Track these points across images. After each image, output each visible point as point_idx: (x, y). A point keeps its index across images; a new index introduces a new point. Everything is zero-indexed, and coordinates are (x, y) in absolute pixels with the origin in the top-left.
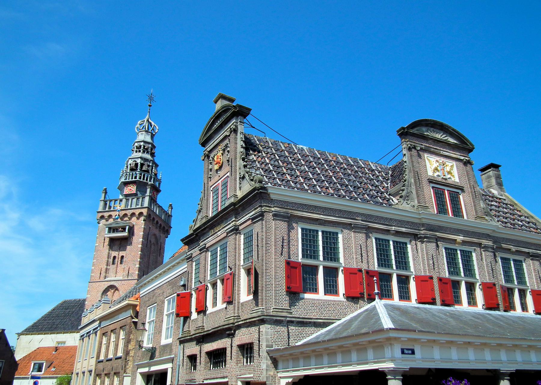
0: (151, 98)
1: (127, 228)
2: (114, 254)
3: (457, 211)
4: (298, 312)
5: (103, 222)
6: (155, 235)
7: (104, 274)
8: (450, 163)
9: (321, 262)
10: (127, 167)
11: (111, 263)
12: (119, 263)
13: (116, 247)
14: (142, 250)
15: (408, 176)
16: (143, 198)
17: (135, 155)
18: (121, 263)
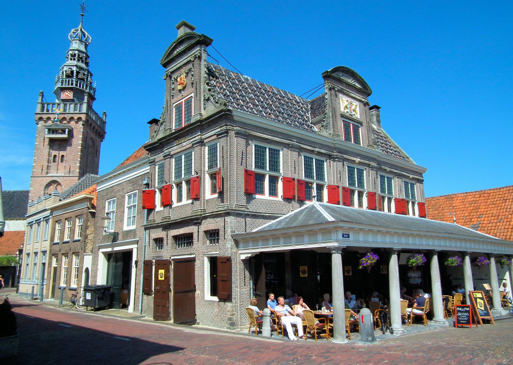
0: (83, 8)
1: (67, 131)
2: (54, 153)
3: (357, 140)
4: (252, 207)
5: (41, 123)
6: (92, 138)
7: (46, 171)
8: (355, 103)
9: (267, 172)
10: (63, 73)
11: (52, 161)
12: (60, 161)
13: (56, 147)
14: (82, 151)
15: (328, 111)
16: (81, 104)
17: (69, 62)
18: (62, 161)
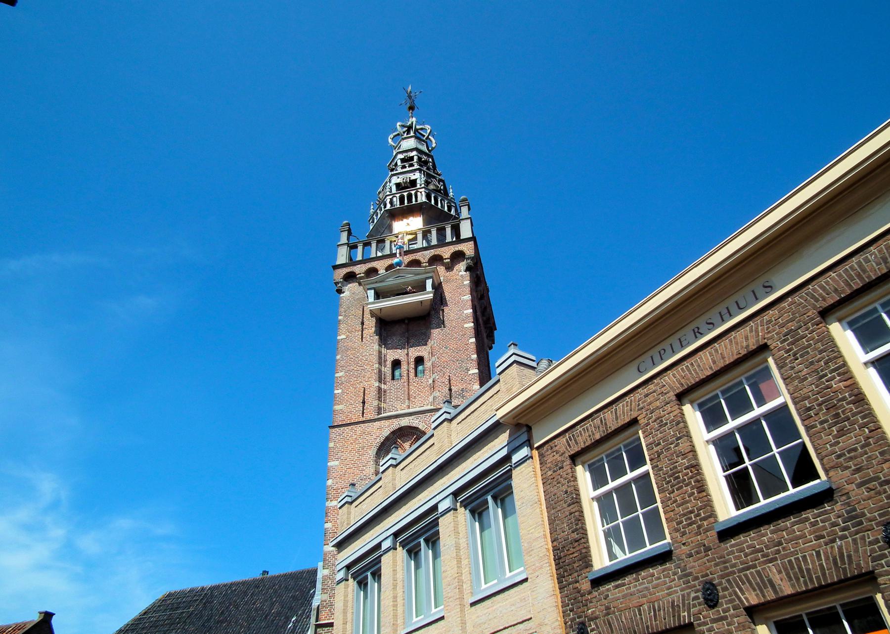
2: (392, 355)
5: (351, 289)
7: (376, 403)
11: (389, 377)
13: (396, 339)
